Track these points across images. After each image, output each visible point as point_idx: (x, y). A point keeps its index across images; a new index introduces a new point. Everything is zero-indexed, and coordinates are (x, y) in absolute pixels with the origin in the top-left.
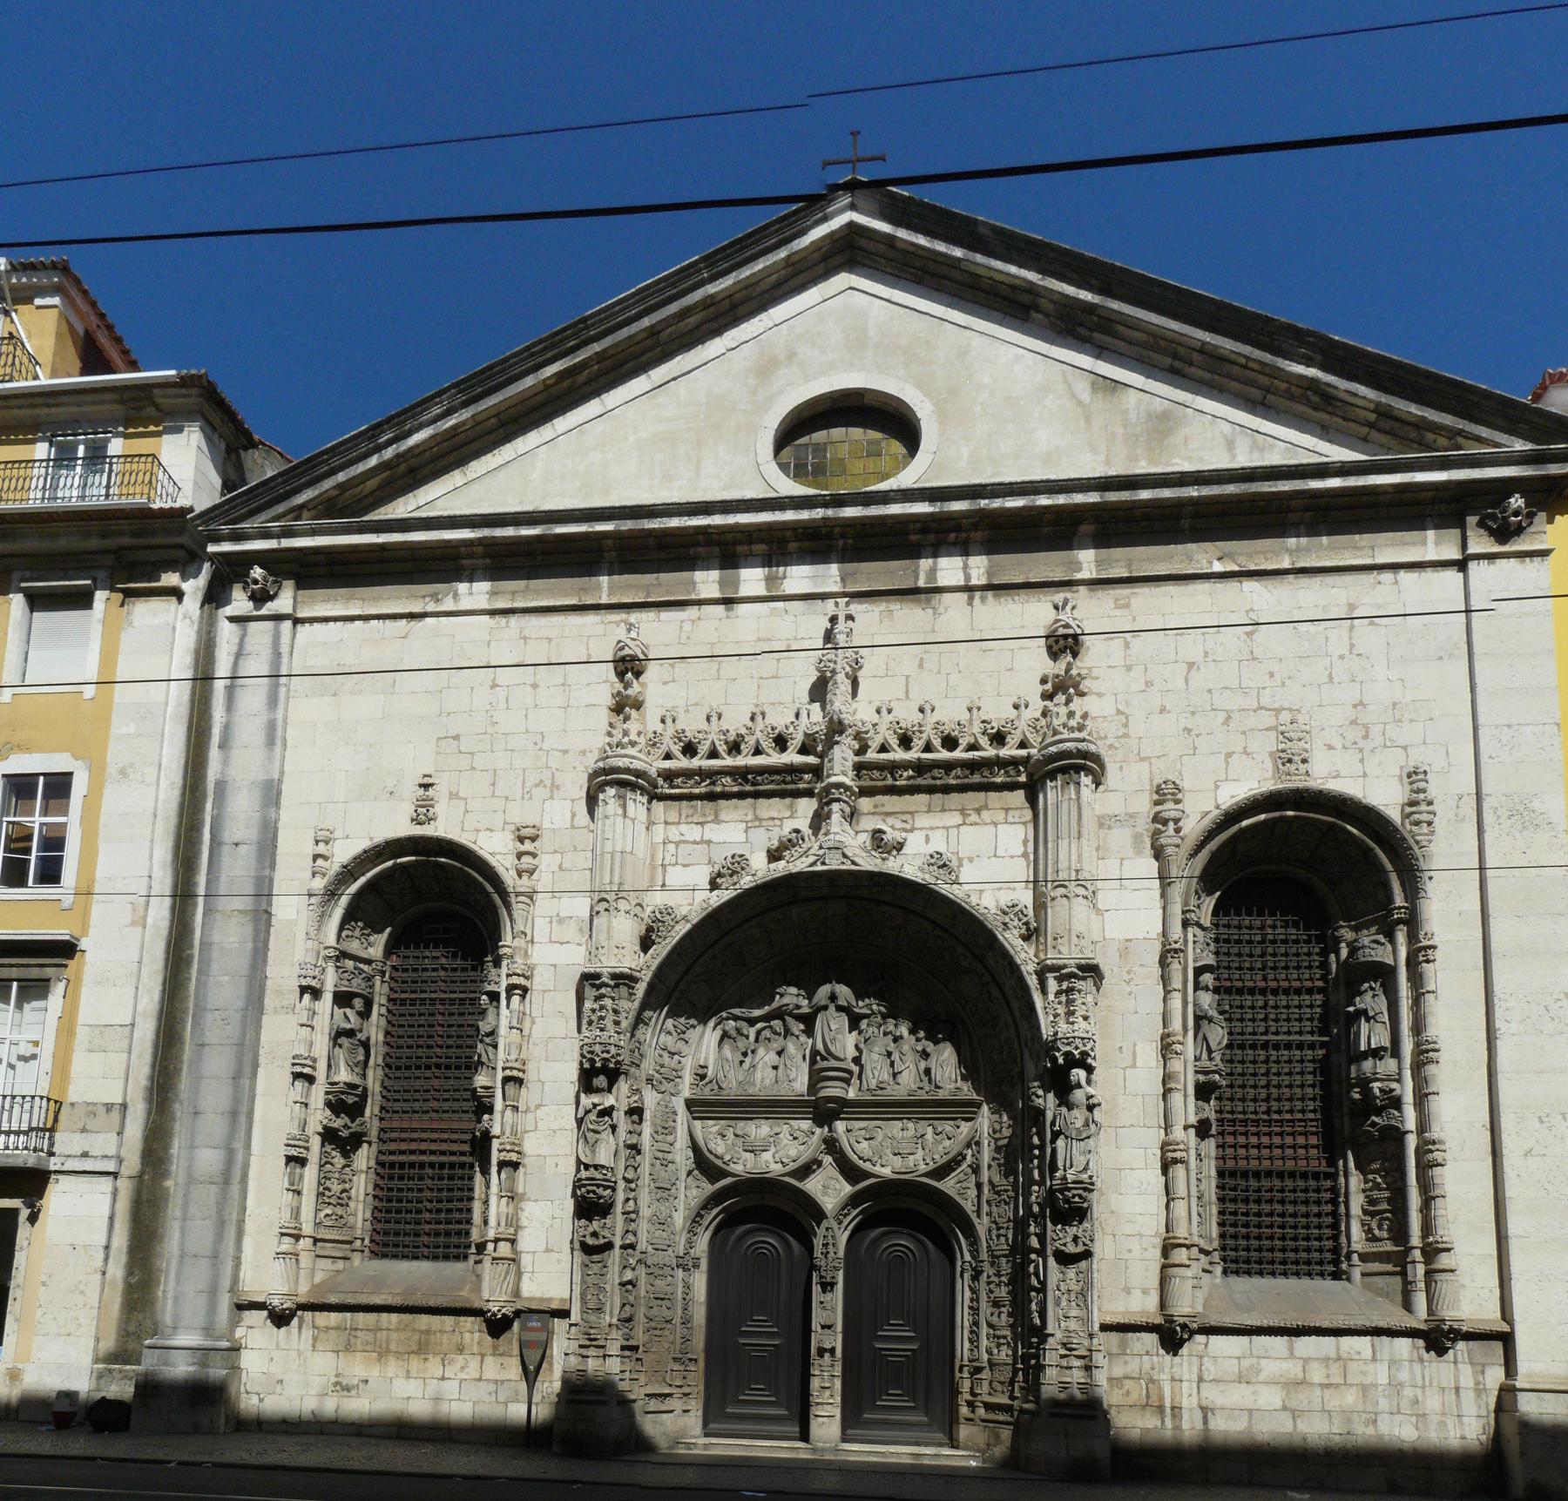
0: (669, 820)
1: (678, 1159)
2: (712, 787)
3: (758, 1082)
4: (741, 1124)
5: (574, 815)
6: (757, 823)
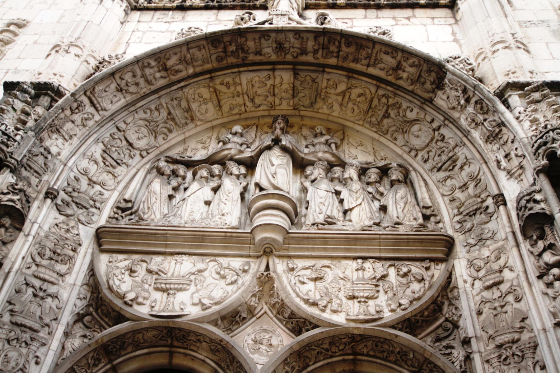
0: (141, 19)
1: (64, 295)
2: (183, 3)
3: (186, 217)
4: (158, 259)
5: (62, 16)
6: (218, 22)
